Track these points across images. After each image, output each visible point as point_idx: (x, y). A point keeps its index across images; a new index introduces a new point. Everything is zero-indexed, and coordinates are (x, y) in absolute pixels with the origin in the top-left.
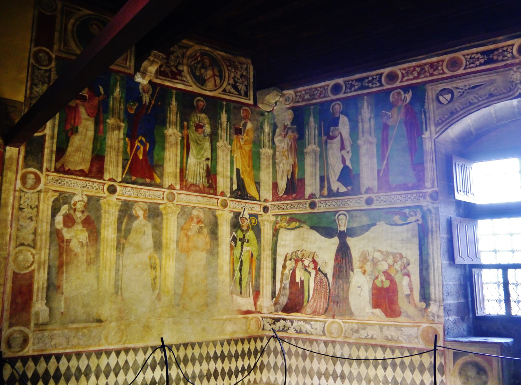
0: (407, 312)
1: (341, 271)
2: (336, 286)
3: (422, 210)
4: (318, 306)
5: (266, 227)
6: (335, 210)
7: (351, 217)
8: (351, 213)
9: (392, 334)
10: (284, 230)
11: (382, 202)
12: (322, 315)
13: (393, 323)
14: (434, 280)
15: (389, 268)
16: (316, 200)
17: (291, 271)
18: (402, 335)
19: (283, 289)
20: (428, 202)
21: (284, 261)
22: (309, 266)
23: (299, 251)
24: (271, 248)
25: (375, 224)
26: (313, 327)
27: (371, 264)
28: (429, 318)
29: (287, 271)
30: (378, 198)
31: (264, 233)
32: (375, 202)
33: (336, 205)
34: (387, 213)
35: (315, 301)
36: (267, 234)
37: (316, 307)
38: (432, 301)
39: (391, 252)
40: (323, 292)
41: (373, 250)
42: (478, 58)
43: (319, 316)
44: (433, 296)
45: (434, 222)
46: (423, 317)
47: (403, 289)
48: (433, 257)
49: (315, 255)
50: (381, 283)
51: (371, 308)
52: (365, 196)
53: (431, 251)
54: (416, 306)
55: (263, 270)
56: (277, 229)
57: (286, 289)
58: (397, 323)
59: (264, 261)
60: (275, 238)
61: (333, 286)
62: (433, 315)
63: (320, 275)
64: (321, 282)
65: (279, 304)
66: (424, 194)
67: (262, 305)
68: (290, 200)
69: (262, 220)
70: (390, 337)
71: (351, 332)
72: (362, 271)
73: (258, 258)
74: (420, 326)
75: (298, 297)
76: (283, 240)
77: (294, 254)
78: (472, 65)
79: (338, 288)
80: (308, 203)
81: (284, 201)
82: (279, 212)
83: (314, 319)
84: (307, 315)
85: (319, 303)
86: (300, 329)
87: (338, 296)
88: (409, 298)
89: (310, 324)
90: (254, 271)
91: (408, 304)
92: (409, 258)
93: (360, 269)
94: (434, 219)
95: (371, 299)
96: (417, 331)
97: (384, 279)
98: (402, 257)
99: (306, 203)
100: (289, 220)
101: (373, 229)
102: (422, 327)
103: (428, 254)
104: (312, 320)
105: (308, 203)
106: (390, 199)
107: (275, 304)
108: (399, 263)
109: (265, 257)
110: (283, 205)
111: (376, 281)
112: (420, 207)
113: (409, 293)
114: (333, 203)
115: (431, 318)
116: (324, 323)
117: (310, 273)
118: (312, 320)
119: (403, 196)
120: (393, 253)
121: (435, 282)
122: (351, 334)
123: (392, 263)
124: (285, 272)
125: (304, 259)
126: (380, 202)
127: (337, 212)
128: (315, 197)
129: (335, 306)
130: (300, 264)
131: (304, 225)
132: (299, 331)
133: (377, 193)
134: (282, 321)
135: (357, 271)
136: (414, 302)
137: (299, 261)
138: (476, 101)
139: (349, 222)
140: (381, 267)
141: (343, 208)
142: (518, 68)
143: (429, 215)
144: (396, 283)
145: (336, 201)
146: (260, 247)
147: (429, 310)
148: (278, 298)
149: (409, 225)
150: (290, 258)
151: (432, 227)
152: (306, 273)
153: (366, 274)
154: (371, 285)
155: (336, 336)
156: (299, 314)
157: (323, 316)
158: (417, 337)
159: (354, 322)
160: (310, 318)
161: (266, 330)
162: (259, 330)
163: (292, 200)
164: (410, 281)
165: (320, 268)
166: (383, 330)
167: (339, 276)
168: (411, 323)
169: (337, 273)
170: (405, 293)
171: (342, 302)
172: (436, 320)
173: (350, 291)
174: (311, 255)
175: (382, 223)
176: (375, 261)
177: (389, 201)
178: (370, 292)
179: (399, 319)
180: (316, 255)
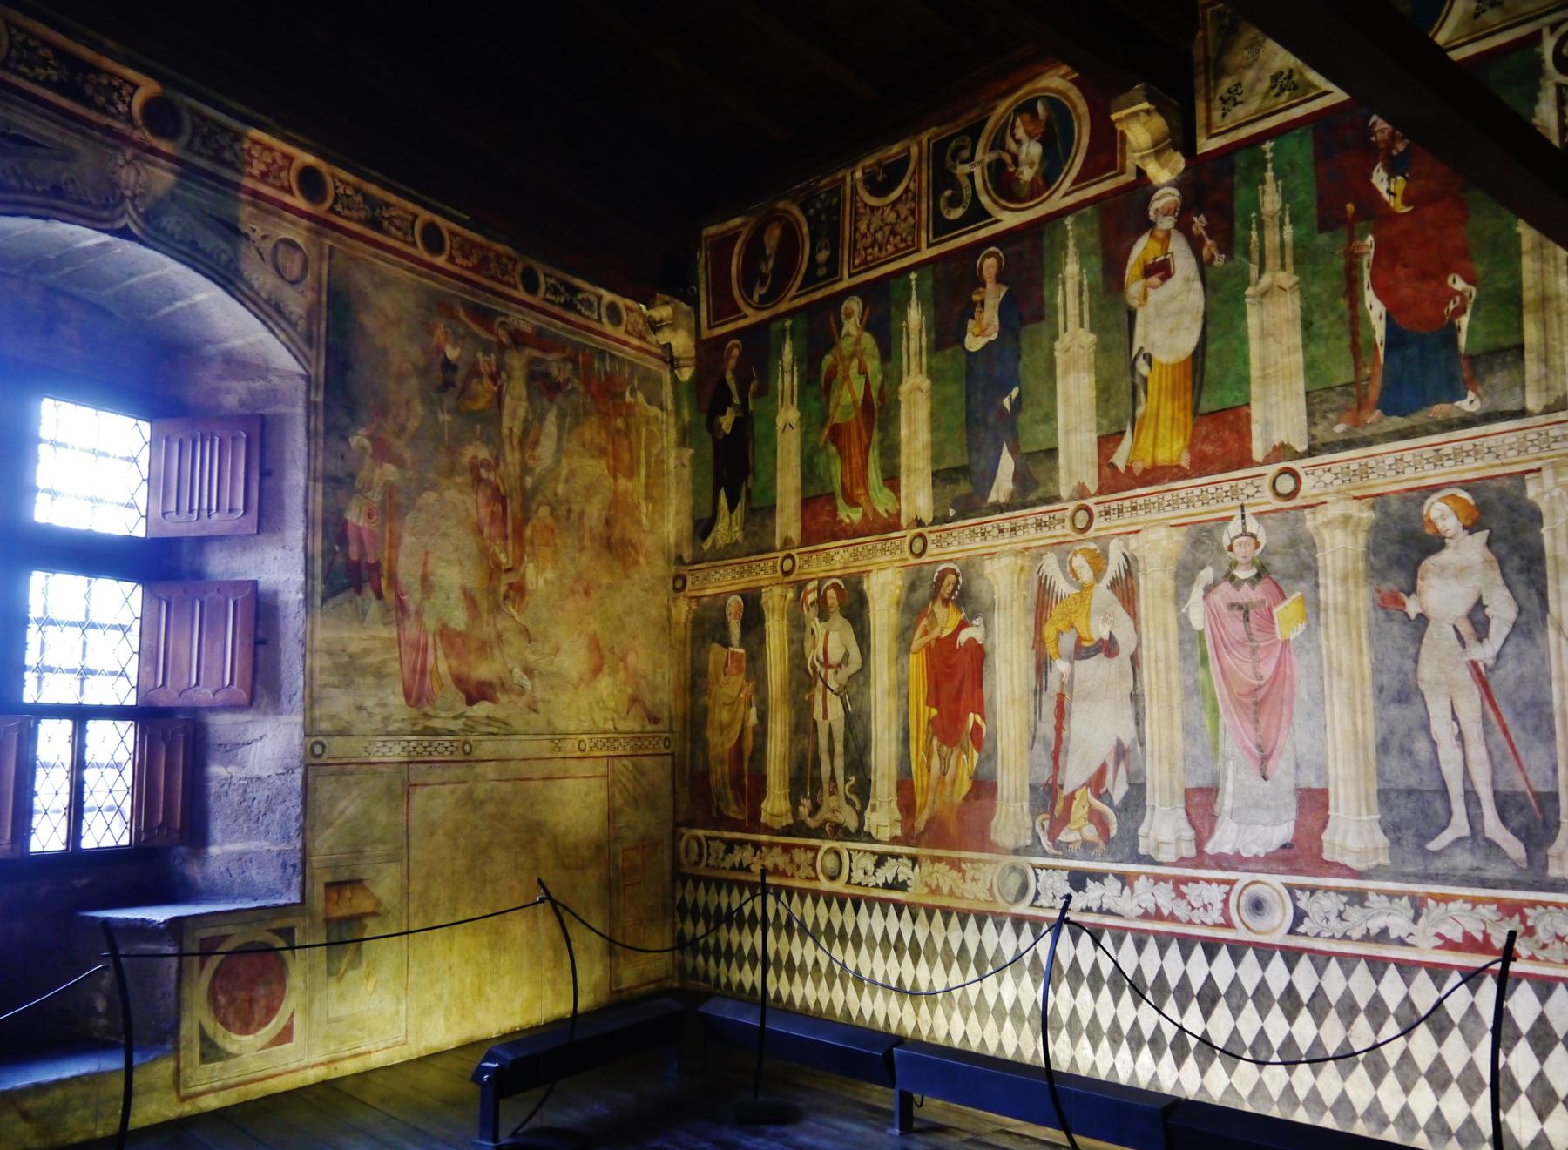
42: (46, 59)
78: (24, 69)
138: (13, 183)
142: (136, 157)
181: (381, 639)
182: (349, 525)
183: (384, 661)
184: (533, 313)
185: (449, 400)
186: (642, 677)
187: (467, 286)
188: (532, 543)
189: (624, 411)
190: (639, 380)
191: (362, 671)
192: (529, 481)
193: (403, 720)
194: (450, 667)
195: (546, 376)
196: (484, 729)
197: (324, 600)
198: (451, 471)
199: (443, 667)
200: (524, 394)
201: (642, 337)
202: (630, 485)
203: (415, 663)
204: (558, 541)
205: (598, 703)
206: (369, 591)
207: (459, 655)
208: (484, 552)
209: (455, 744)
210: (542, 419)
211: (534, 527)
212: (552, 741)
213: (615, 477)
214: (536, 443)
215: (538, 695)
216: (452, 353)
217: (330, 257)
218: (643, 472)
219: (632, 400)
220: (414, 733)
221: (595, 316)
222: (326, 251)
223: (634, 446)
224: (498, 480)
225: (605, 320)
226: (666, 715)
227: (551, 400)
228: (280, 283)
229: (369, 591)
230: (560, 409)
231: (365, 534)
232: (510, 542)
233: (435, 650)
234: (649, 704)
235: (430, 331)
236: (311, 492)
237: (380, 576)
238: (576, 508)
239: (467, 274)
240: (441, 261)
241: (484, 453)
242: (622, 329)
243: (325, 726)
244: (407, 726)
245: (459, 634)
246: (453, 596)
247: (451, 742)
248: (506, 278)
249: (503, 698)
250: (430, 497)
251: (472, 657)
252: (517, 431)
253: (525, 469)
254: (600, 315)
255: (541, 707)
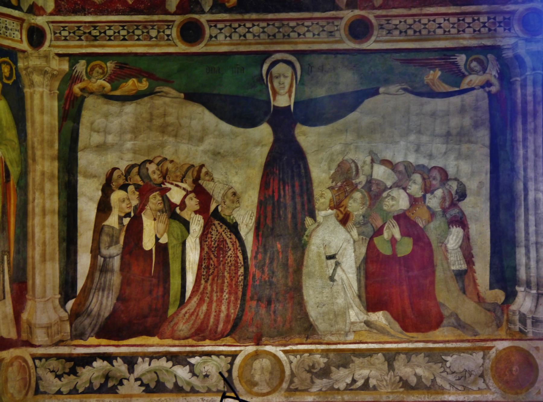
0: (457, 315)
1: (280, 216)
2: (264, 259)
3: (499, 58)
4: (213, 314)
5: (39, 89)
6: (261, 48)
7: (307, 70)
8: (308, 58)
9: (419, 371)
10: (100, 101)
11: (397, 32)
12: (223, 335)
13: (421, 345)
14: (527, 233)
15: (412, 205)
16: (203, 18)
17: (126, 221)
18: (444, 374)
19: (101, 271)
20: (518, 37)
21: (103, 190)
22: (183, 205)
23: (151, 162)
24: (56, 152)
25: (375, 92)
26: (197, 371)
27: (363, 197)
28: (512, 326)
29: (113, 221)
30: (383, 22)
31: (32, 109)
32: (375, 33)
33: (262, 35)
34: (408, 62)
35: (201, 301)
36: (42, 112)
37: (208, 314)
38: (519, 286)
39: (419, 166)
40: (226, 274)
41: (368, 159)
43: (215, 340)
44: (522, 274)
45: (530, 90)
46: (499, 326)
47: (447, 259)
48: (525, 177)
49: (202, 175)
50: (390, 245)
51: (365, 312)
52: (349, 15)
53: (520, 162)
54: (480, 300)
55: (33, 219)
56: (76, 98)
57: (112, 271)
58: (431, 345)
59: (34, 193)
60: (69, 124)
61: (256, 257)
62: (523, 319)
63: (218, 228)
64: (221, 247)
65: (89, 315)
66: (507, 16)
67: (33, 322)
68: (118, 12)
69: (26, 68)
70: (413, 381)
71: (309, 375)
72: (337, 217)
73: (22, 183)
74: (490, 348)
75: (150, 292)
76: (98, 132)
77: (136, 170)
79: (271, 262)
80: (176, 23)
81: (95, 13)
82: (81, 47)
83: (200, 349)
84: (179, 339)
85: (214, 305)
86: (158, 382)
87: (271, 284)
88: (463, 282)
89: (189, 364)
90: (12, 220)
91: (461, 293)
92: (464, 180)
93: (335, 211)
94: (529, 83)
95: (363, 289)
96: (481, 361)
97: (398, 236)
98: (445, 177)
99: (169, 24)
100: (114, 73)
101: (369, 103)
102: (494, 350)
103: (513, 170)
104: (193, 354)
105: (176, 23)
106: (416, 27)
107: (74, 316)
108: (439, 193)
109: (38, 179)
110: (95, 28)
111: (376, 240)
112: (496, 50)
113: (464, 267)
114: (256, 29)
115: (518, 326)
116: (229, 359)
117: (186, 224)
118: (193, 354)
119: (453, 20)
120: (423, 166)
121: (527, 239)
122: (309, 381)
123: (419, 194)
124: (106, 223)
125: (168, 185)
126: (389, 32)
127: (268, 54)
128: (198, 9)
129: (263, 311)
130: (155, 200)
131: (166, 89)
132: (152, 385)
133: (380, 8)
134: (98, 364)
135: (326, 217)
136: (476, 289)
137: (152, 190)
139: (301, 83)
140: (391, 203)
141: (283, 43)
143: (518, 70)
144: (429, 244)
145: (264, 24)
146: (26, 152)
147: (513, 307)
148: (86, 299)
149: (465, 96)
150: (121, 182)
151: (525, 103)
152: (176, 226)
153: (350, 224)
154: (364, 250)
155: (265, 391)
156: (155, 340)
157: (229, 340)
158: (482, 376)
159: (317, 350)
160: (188, 349)
161: (45, 393)
162: (27, 394)
163: (124, 13)
164: (467, 238)
165: (216, 209)
166: (396, 365)
167: (272, 229)
168: (468, 341)
169: (269, 222)
170: (453, 268)
171: (281, 298)
172: (530, 329)
173: (305, 270)
174: (190, 173)
175: (393, 88)
176: (374, 188)
177: (415, 32)
178: (359, 269)
179: (439, 334)
180: (207, 173)
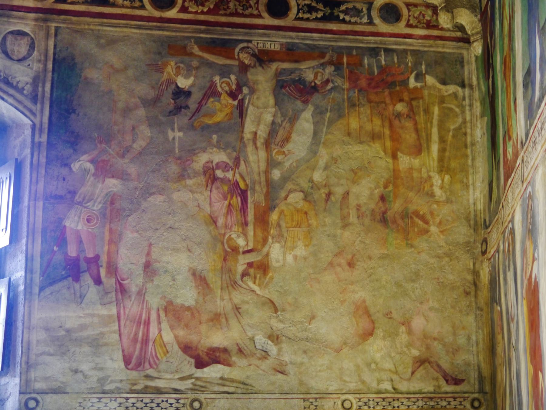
181: (98, 315)
182: (68, 230)
183: (102, 334)
184: (281, 33)
185: (182, 120)
186: (435, 339)
187: (203, 27)
188: (279, 225)
189: (406, 96)
190: (427, 65)
191: (79, 342)
192: (276, 174)
193: (121, 381)
194: (176, 337)
195: (301, 81)
196: (216, 388)
197: (42, 289)
198: (181, 177)
199: (168, 336)
200: (272, 101)
201: (429, 25)
202: (416, 162)
203: (136, 334)
204: (313, 222)
205: (368, 365)
206: (87, 279)
207: (187, 326)
208: (218, 239)
209: (182, 401)
210: (294, 119)
211: (282, 212)
212: (304, 400)
213: (394, 157)
214: (287, 139)
215: (286, 358)
216: (183, 83)
217: (56, 35)
218: (435, 148)
219: (419, 85)
220: (132, 392)
221: (365, 20)
222: (53, 31)
223: (421, 126)
224: (237, 177)
225: (377, 20)
226: (473, 375)
227: (306, 102)
228: (8, 63)
229: (87, 279)
230: (317, 107)
231: (84, 238)
232: (250, 229)
233: (159, 323)
234: (445, 366)
235: (160, 70)
236: (32, 210)
237: (98, 267)
238: (339, 191)
239: (202, 17)
240: (172, 13)
241: (220, 157)
242: (403, 23)
243: (39, 385)
244: (127, 387)
245: (189, 308)
246: (179, 278)
247: (177, 400)
248: (247, 12)
249: (240, 362)
250: (157, 200)
251: (204, 328)
252: (263, 133)
253: (271, 164)
254: (370, 17)
255: (290, 369)
